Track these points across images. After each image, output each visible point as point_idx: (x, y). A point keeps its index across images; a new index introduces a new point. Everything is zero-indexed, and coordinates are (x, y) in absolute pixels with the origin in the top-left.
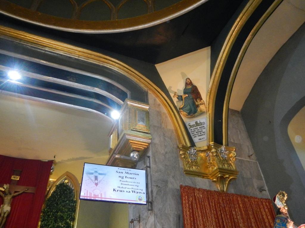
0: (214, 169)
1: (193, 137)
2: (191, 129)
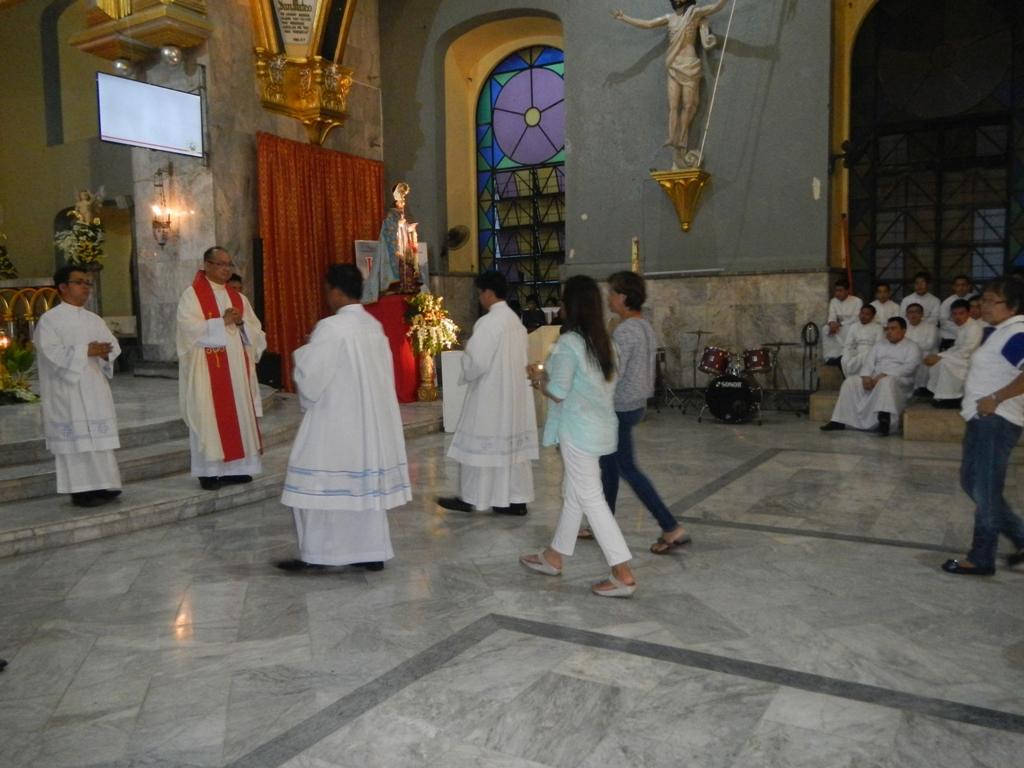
0: (311, 106)
1: (282, 30)
2: (285, 12)
